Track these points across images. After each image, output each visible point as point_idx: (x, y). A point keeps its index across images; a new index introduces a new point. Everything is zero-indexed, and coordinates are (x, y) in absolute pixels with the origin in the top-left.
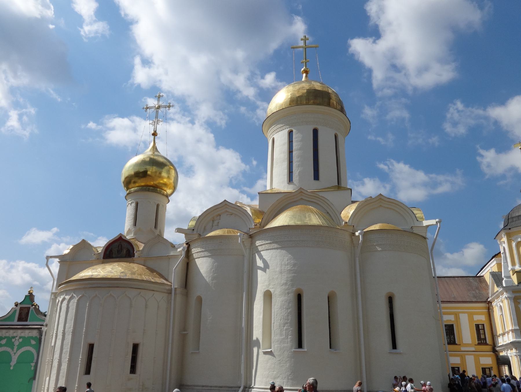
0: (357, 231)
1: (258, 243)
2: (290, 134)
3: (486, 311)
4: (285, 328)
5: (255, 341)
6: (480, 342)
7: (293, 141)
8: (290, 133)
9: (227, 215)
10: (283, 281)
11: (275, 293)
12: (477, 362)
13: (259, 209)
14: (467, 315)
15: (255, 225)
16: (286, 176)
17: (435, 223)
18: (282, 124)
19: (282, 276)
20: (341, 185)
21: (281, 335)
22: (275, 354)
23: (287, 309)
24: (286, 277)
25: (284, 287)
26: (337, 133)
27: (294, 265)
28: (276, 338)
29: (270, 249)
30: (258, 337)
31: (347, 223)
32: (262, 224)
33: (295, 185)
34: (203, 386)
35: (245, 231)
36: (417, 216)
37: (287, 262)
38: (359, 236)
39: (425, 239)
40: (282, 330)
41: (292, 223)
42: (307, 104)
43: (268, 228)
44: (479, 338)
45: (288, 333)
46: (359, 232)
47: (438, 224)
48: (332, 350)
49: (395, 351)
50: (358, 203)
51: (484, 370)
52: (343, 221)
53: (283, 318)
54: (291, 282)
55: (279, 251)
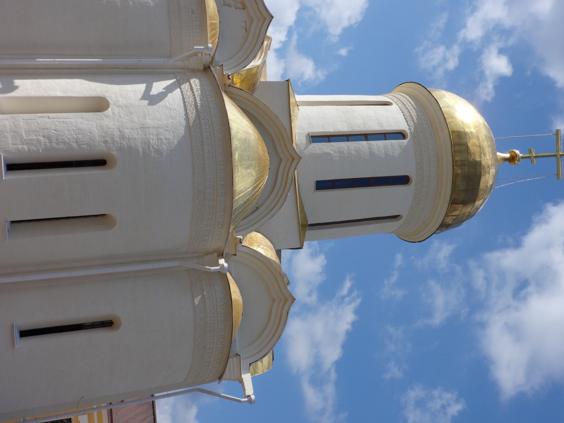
0: (226, 262)
1: (195, 82)
2: (400, 135)
4: (42, 139)
5: (13, 83)
7: (386, 140)
8: (401, 135)
9: (246, 22)
10: (127, 132)
11: (104, 118)
13: (259, 82)
15: (229, 76)
16: (321, 130)
17: (247, 394)
18: (417, 119)
19: (137, 129)
20: (309, 230)
21: (28, 132)
23: (77, 142)
24: (136, 137)
25: (117, 133)
27: (158, 151)
28: (21, 123)
29: (185, 106)
30: (20, 89)
31: (241, 242)
32: (231, 89)
33: (306, 147)
35: (217, 58)
36: (259, 363)
37: (163, 137)
38: (217, 264)
39: (219, 379)
40: (37, 134)
41: (235, 143)
42: (454, 162)
43: (223, 101)
45: (32, 144)
46: (226, 265)
47: (246, 399)
48: (8, 225)
49: (17, 334)
50: (277, 261)
52: (244, 236)
53: (59, 135)
54: (128, 146)
55: (184, 122)
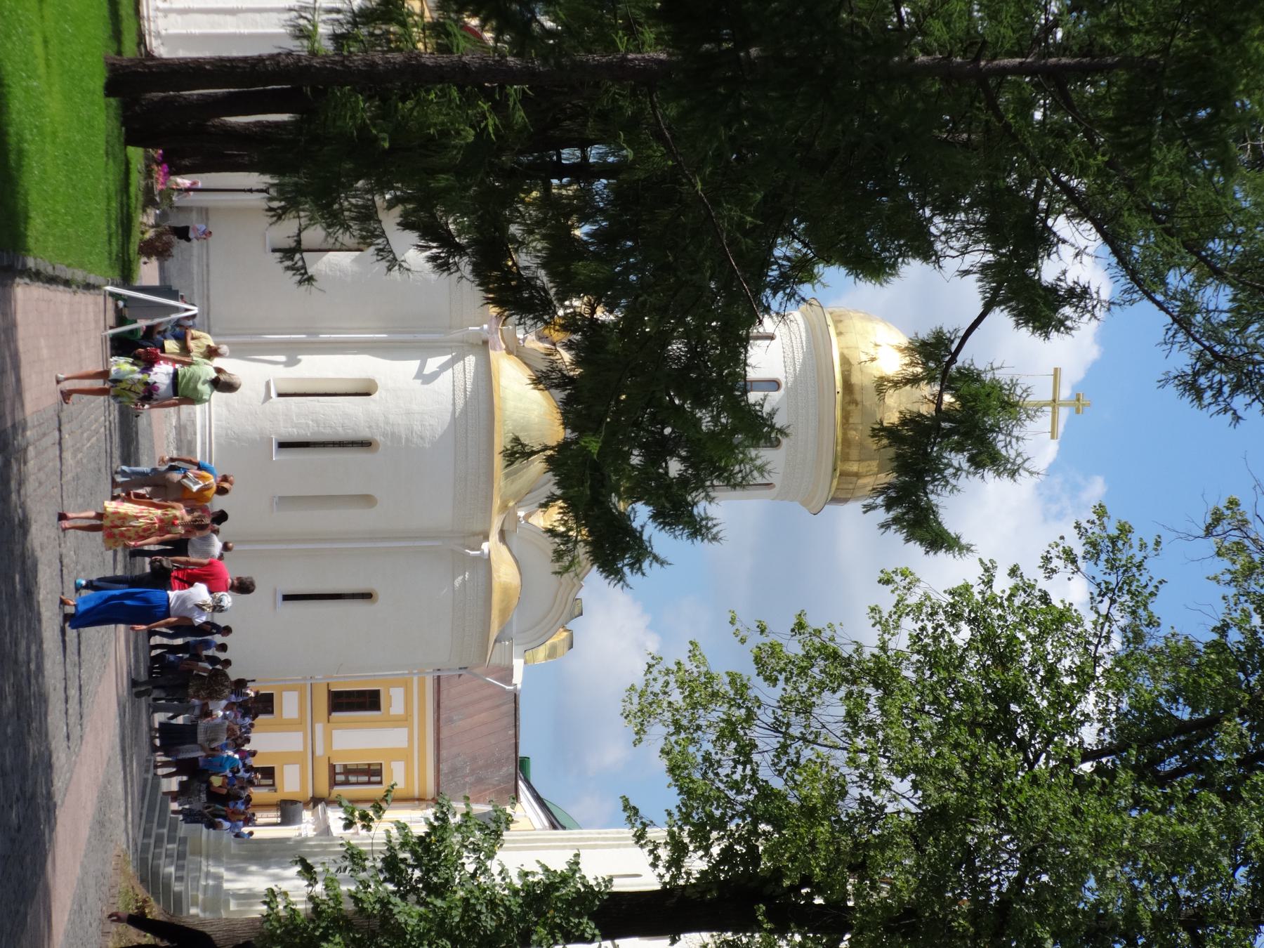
3: (416, 794)
6: (338, 770)
12: (290, 758)
14: (405, 745)
22: (267, 404)
26: (773, 490)
29: (454, 390)
34: (208, 266)
38: (479, 549)
44: (348, 771)
49: (280, 598)
51: (269, 773)
55: (450, 408)
